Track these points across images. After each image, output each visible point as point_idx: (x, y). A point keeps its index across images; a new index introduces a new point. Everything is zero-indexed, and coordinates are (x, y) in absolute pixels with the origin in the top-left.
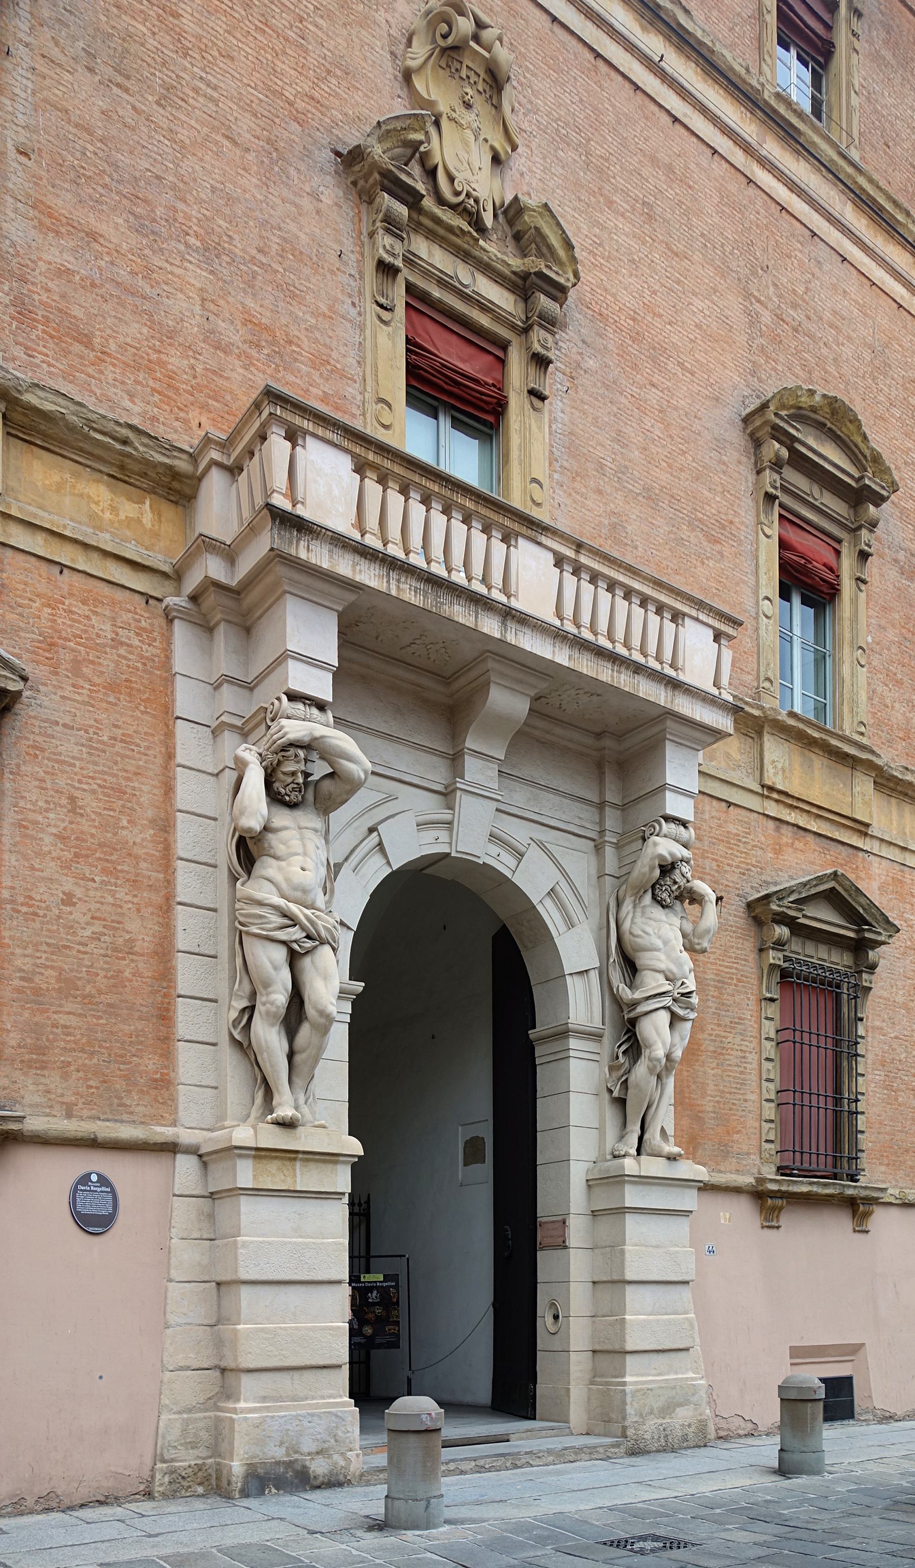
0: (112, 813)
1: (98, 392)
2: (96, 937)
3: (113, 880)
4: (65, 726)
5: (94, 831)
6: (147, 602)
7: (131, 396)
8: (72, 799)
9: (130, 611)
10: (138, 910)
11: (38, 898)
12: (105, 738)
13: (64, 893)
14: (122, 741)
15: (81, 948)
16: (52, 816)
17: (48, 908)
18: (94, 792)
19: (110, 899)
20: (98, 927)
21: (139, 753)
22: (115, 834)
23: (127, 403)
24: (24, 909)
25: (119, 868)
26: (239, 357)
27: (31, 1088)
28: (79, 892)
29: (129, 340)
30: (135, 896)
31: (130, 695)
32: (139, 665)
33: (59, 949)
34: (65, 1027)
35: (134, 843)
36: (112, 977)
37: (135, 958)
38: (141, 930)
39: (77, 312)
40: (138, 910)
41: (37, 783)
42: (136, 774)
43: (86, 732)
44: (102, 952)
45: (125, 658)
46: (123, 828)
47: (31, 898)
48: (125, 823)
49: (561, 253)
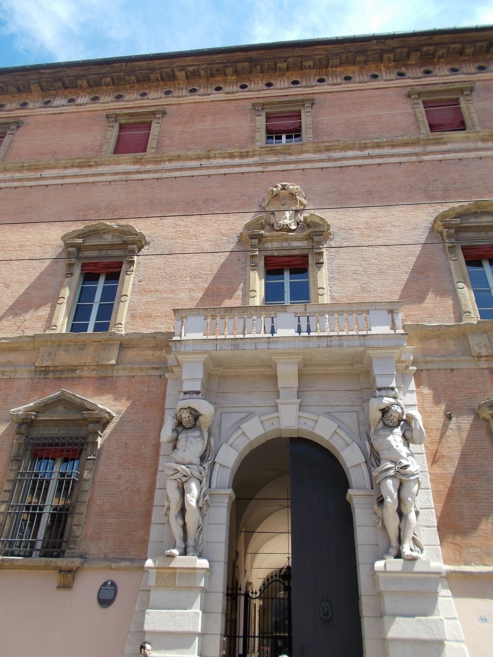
2: (127, 489)
5: (132, 452)
8: (126, 444)
15: (120, 493)
16: (118, 450)
17: (111, 482)
18: (134, 439)
20: (128, 485)
22: (139, 451)
24: (103, 483)
27: (94, 548)
31: (151, 406)
34: (110, 523)
36: (131, 502)
42: (150, 430)
44: (128, 494)
47: (106, 479)
49: (321, 223)
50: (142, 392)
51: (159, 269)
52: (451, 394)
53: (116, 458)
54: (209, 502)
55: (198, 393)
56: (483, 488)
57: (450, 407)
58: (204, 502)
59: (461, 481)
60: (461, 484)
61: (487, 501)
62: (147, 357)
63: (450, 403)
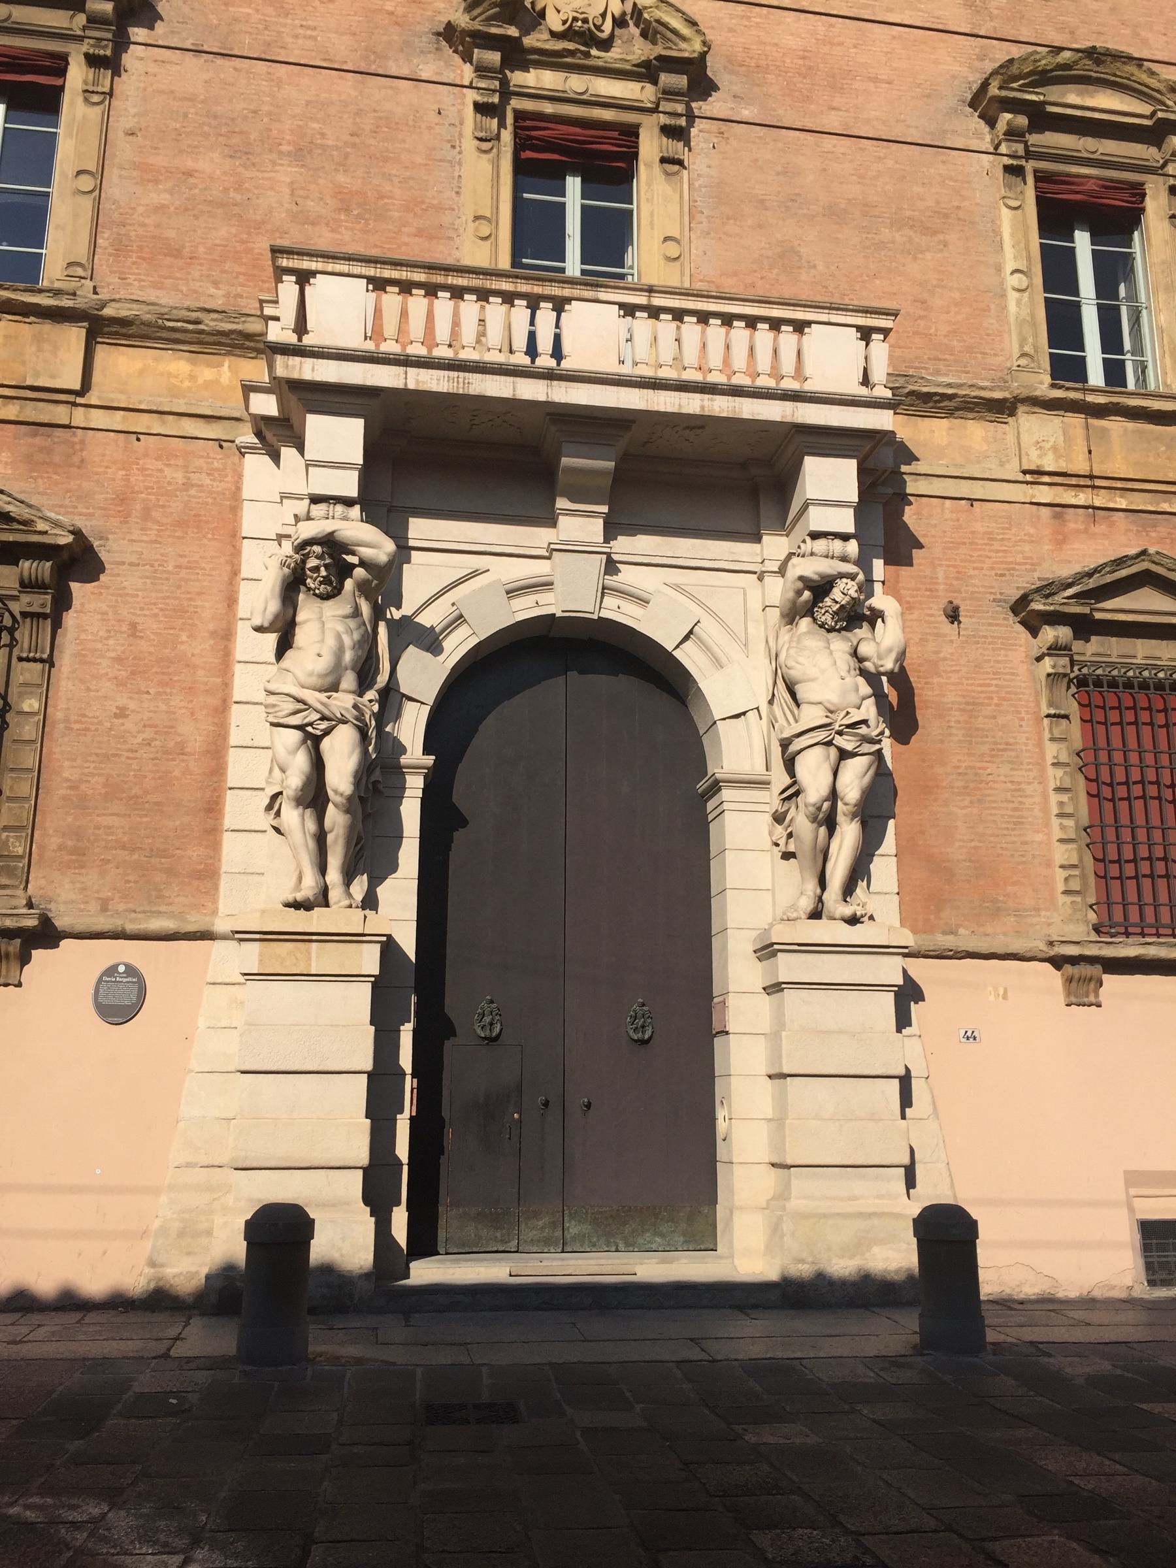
0: (172, 632)
1: (184, 289)
3: (168, 690)
4: (131, 564)
5: (152, 649)
6: (221, 447)
7: (216, 284)
8: (133, 626)
9: (202, 457)
10: (192, 714)
11: (91, 715)
12: (170, 568)
13: (117, 708)
14: (187, 568)
15: (131, 755)
16: (111, 642)
17: (100, 723)
18: (156, 615)
19: (163, 707)
20: (149, 734)
21: (204, 575)
22: (174, 649)
23: (212, 291)
24: (76, 726)
25: (176, 678)
26: (327, 225)
27: (67, 886)
28: (132, 705)
29: (217, 242)
30: (191, 701)
31: (198, 527)
32: (210, 500)
33: (107, 758)
34: (109, 827)
35: (193, 655)
36: (160, 778)
37: (185, 757)
38: (194, 734)
39: (171, 234)
40: (192, 714)
41: (99, 617)
43: (152, 566)
44: (152, 756)
45: (194, 497)
46: (182, 643)
47: (84, 716)
48: (184, 638)
50: (169, 483)
51: (192, 99)
52: (961, 561)
53: (105, 663)
54: (380, 787)
55: (348, 502)
56: (1002, 778)
57: (954, 592)
58: (370, 786)
59: (959, 761)
60: (958, 767)
61: (1005, 805)
62: (173, 380)
63: (955, 583)
